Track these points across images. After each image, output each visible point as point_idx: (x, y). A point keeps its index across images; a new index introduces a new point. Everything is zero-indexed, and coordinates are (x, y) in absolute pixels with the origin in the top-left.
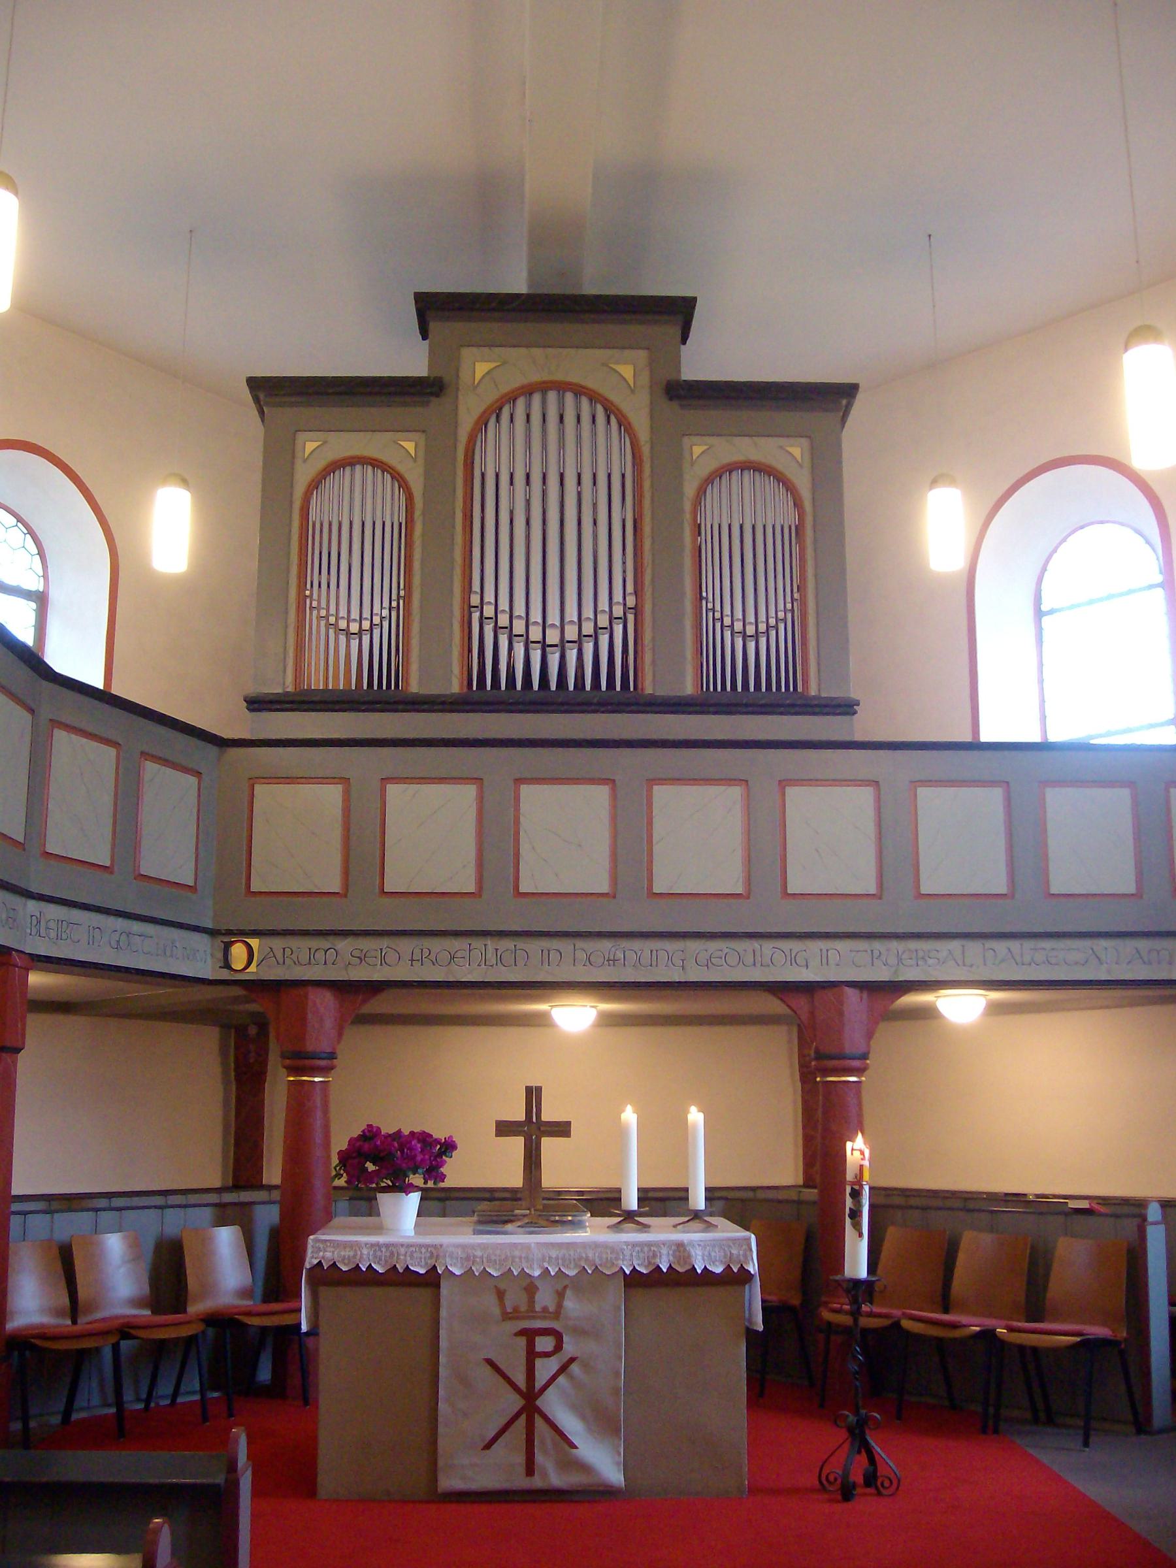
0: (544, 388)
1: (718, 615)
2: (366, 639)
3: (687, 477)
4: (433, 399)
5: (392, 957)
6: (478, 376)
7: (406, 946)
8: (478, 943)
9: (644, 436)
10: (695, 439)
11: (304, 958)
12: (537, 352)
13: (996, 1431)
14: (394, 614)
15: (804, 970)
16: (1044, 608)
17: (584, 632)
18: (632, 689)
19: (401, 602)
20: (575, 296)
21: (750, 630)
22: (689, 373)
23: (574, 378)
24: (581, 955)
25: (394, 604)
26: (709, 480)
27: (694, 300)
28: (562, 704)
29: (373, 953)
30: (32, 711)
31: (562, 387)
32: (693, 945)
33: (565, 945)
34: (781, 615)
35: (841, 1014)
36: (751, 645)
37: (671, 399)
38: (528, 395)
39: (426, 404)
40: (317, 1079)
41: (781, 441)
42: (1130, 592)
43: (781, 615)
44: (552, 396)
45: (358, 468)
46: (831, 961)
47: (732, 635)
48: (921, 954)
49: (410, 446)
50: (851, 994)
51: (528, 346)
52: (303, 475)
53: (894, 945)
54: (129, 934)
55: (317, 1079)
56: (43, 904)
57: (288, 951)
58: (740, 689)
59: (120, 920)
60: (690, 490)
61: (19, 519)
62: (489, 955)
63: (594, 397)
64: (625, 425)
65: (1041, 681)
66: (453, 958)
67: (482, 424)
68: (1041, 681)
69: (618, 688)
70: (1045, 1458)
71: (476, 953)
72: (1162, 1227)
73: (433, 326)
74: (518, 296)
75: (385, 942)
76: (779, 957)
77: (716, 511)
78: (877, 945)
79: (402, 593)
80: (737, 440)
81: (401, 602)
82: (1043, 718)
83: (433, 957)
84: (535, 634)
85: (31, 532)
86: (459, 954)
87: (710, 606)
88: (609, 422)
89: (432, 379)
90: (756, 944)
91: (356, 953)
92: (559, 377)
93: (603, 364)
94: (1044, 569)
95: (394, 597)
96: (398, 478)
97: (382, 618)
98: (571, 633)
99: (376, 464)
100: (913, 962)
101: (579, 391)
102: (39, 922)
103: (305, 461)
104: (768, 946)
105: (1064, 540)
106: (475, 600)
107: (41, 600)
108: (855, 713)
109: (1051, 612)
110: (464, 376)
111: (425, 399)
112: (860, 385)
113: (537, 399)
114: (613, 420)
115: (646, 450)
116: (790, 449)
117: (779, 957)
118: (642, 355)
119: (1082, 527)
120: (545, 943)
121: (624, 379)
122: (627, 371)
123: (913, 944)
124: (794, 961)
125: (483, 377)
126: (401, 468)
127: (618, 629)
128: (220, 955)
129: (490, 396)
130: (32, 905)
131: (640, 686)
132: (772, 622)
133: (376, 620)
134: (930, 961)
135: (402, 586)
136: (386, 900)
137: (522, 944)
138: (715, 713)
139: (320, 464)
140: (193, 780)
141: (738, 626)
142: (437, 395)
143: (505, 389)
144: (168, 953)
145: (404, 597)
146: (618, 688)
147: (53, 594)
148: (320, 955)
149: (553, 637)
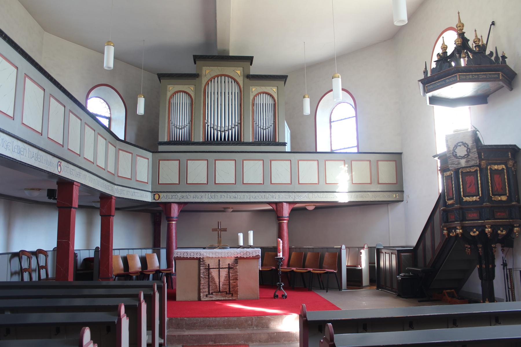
0: (221, 75)
1: (258, 125)
2: (183, 130)
3: (251, 95)
5: (189, 197)
6: (207, 73)
7: (192, 194)
8: (207, 194)
9: (242, 86)
10: (253, 87)
11: (171, 198)
13: (311, 291)
14: (189, 124)
15: (275, 199)
16: (332, 121)
17: (229, 128)
19: (190, 122)
21: (264, 128)
22: (252, 73)
24: (228, 196)
25: (189, 122)
26: (256, 96)
27: (253, 57)
28: (225, 144)
29: (185, 196)
30: (115, 147)
31: (225, 76)
32: (251, 194)
33: (225, 194)
34: (271, 125)
35: (283, 208)
36: (265, 131)
37: (248, 78)
39: (195, 79)
40: (173, 223)
41: (272, 87)
42: (349, 118)
43: (271, 125)
44: (223, 77)
45: (181, 93)
46: (281, 197)
47: (261, 129)
48: (299, 196)
49: (192, 89)
50: (285, 204)
51: (217, 66)
52: (169, 94)
53: (294, 194)
54: (134, 192)
55: (173, 223)
56: (118, 186)
57: (167, 196)
58: (262, 140)
59: (133, 189)
60: (251, 98)
61: (105, 101)
62: (209, 196)
63: (232, 78)
64: (238, 83)
65: (331, 137)
66: (202, 197)
67: (207, 84)
68: (331, 137)
69: (237, 140)
70: (319, 294)
71: (207, 196)
72: (345, 250)
73: (197, 62)
74: (215, 56)
75: (188, 193)
76: (270, 196)
77: (258, 100)
78: (290, 194)
79: (191, 120)
80: (262, 87)
81: (190, 122)
82: (331, 145)
83: (197, 197)
84: (219, 129)
85: (107, 104)
86: (203, 196)
87: (256, 123)
88: (235, 83)
90: (265, 194)
91: (181, 196)
92: (224, 73)
94: (332, 112)
95: (189, 121)
96: (189, 95)
97: (186, 125)
98: (226, 129)
100: (298, 198)
101: (229, 76)
102: (117, 190)
104: (267, 194)
105: (336, 106)
106: (206, 121)
107: (110, 119)
108: (286, 145)
109: (333, 122)
110: (204, 73)
112: (288, 76)
114: (235, 82)
115: (242, 89)
116: (273, 89)
117: (270, 196)
119: (340, 103)
120: (221, 194)
122: (239, 72)
123: (298, 194)
124: (273, 197)
126: (190, 93)
127: (237, 127)
128: (153, 197)
129: (209, 77)
130: (116, 186)
132: (269, 126)
133: (185, 126)
134: (301, 197)
135: (191, 119)
136: (187, 185)
137: (216, 194)
139: (173, 92)
140: (147, 160)
141: (262, 127)
142: (198, 77)
143: (212, 76)
144: (142, 197)
146: (237, 140)
147: (112, 117)
148: (174, 196)
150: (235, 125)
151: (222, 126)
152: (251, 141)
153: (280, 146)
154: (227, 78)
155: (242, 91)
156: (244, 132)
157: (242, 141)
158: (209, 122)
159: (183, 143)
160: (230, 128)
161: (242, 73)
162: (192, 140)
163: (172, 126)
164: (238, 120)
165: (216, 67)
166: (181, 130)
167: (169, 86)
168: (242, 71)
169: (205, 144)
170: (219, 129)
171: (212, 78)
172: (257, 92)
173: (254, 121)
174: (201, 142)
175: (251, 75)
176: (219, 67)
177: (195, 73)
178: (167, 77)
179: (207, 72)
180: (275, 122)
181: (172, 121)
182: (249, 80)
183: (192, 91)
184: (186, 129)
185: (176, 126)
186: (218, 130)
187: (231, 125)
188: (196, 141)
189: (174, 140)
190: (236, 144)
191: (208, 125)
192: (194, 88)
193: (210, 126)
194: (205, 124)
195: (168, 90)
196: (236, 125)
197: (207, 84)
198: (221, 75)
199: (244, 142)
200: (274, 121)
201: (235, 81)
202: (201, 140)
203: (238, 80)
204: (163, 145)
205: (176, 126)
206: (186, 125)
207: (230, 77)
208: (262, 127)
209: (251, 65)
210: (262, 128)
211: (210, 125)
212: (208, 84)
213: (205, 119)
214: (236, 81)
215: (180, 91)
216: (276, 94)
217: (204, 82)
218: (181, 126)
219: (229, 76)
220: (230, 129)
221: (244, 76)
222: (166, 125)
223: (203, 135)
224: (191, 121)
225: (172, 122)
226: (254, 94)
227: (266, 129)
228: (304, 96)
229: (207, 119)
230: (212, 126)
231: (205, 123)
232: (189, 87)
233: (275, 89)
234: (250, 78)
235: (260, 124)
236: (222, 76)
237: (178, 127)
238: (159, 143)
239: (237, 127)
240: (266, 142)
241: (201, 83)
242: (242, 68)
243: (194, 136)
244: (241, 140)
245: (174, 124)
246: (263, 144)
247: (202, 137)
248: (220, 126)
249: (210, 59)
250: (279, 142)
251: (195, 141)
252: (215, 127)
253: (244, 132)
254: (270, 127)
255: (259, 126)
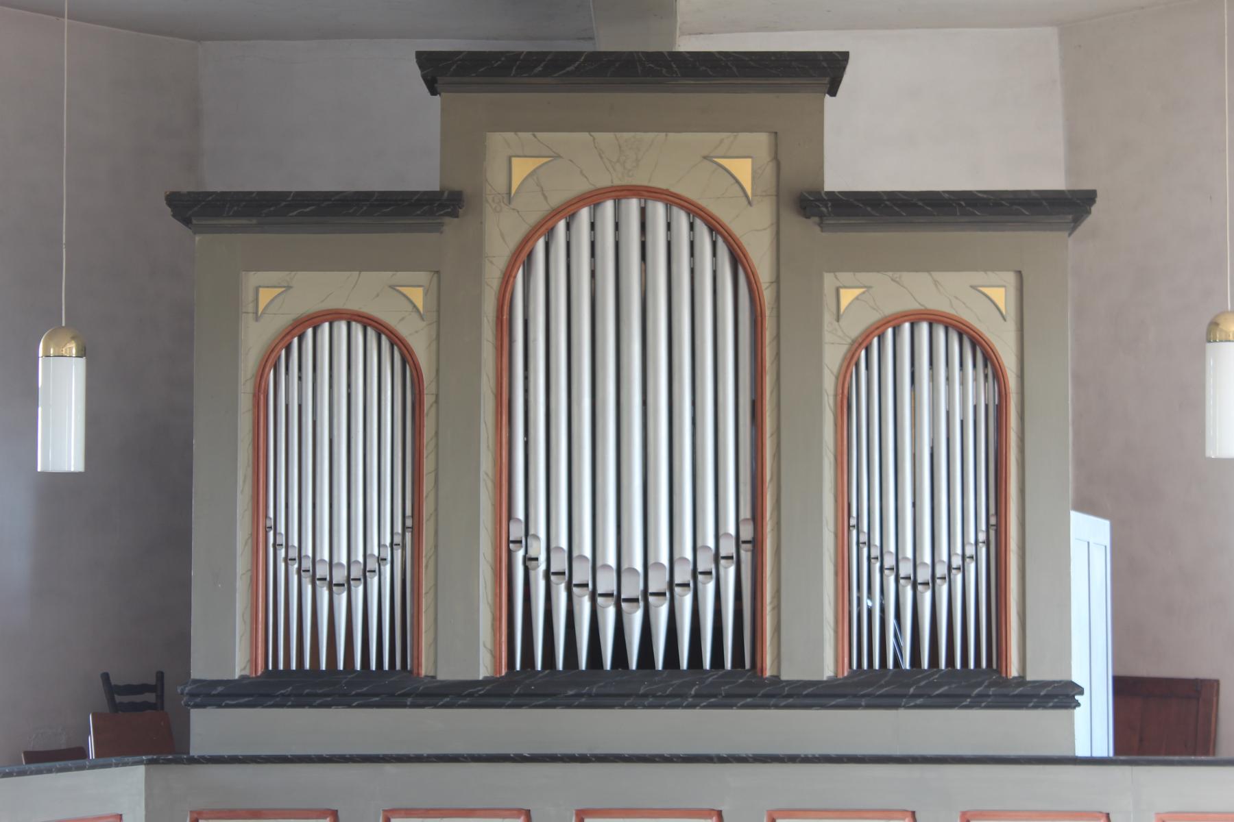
0: (619, 193)
1: (875, 552)
3: (828, 337)
4: (447, 220)
9: (764, 274)
10: (845, 277)
12: (604, 138)
14: (398, 553)
17: (677, 580)
18: (748, 665)
19: (408, 535)
20: (660, 54)
21: (924, 575)
23: (659, 183)
25: (398, 539)
28: (645, 696)
31: (646, 193)
34: (970, 551)
37: (808, 217)
38: (592, 206)
39: (438, 228)
41: (977, 277)
43: (970, 551)
49: (417, 296)
60: (833, 357)
63: (695, 212)
79: (409, 523)
80: (907, 277)
84: (606, 583)
87: (864, 538)
89: (446, 194)
92: (640, 179)
93: (705, 158)
95: (398, 529)
96: (396, 341)
97: (381, 560)
98: (658, 582)
99: (367, 322)
101: (672, 200)
103: (257, 319)
106: (517, 531)
108: (1078, 705)
110: (495, 178)
111: (439, 221)
112: (1099, 194)
113: (609, 206)
115: (767, 295)
118: (761, 140)
121: (737, 182)
122: (743, 169)
125: (522, 183)
126: (403, 330)
129: (535, 211)
131: (759, 665)
132: (957, 561)
133: (372, 564)
138: (868, 707)
141: (906, 569)
142: (454, 214)
143: (557, 199)
145: (412, 528)
146: (728, 665)
149: (632, 588)
150: (717, 558)
151: (625, 566)
152: (828, 672)
153: (1035, 707)
154: (658, 211)
155: (767, 312)
156: (777, 608)
157: (768, 673)
158: (536, 537)
159: (357, 695)
160: (683, 575)
161: (769, 170)
162: (419, 665)
163: (283, 565)
164: (742, 516)
165: (584, 136)
166: (344, 595)
167: (253, 278)
168: (764, 153)
169: (508, 696)
170: (606, 583)
171: (555, 214)
172: (872, 318)
173: (853, 522)
174: (486, 681)
175: (826, 192)
176: (599, 136)
177: (435, 186)
178: (237, 215)
179: (522, 168)
180: (997, 529)
181: (282, 529)
182: (817, 229)
183: (415, 316)
184: (381, 585)
185: (307, 564)
186: (600, 590)
187: (689, 555)
188: (446, 674)
189: (294, 667)
190: (728, 696)
191: (532, 554)
192: (426, 294)
193: (543, 567)
194: (510, 553)
195: (250, 308)
196: (723, 553)
197: (522, 257)
198: (619, 193)
199: (776, 679)
200: (993, 521)
201: (715, 228)
202: (484, 670)
203: (737, 228)
204: (219, 706)
205: (307, 564)
206: (381, 560)
207: (682, 207)
208: (906, 569)
209: (833, 92)
210: (908, 578)
211: (542, 558)
212: (530, 255)
213: (510, 517)
214: (719, 232)
215: (333, 316)
216: (1011, 327)
217: (499, 250)
218: (340, 564)
219: (672, 200)
220: (686, 585)
221: (778, 195)
222: (242, 564)
223: (496, 629)
224: (413, 523)
225: (282, 540)
226: (855, 329)
227: (932, 583)
228: (1214, 324)
229: (520, 513)
230: (559, 563)
231: (509, 542)
232: (392, 287)
233: (1001, 294)
234: (821, 216)
235: (892, 548)
236: (626, 197)
237: (322, 571)
238: (192, 695)
239: (732, 571)
240: (939, 685)
241: (476, 252)
242: (761, 140)
243: (436, 639)
244: (762, 670)
245: (293, 553)
246: (914, 696)
247: (489, 645)
248: (612, 561)
249: (536, 76)
250: (1029, 678)
251: (444, 675)
252: (582, 574)
253: (777, 608)
254: (963, 569)
255: (886, 565)
